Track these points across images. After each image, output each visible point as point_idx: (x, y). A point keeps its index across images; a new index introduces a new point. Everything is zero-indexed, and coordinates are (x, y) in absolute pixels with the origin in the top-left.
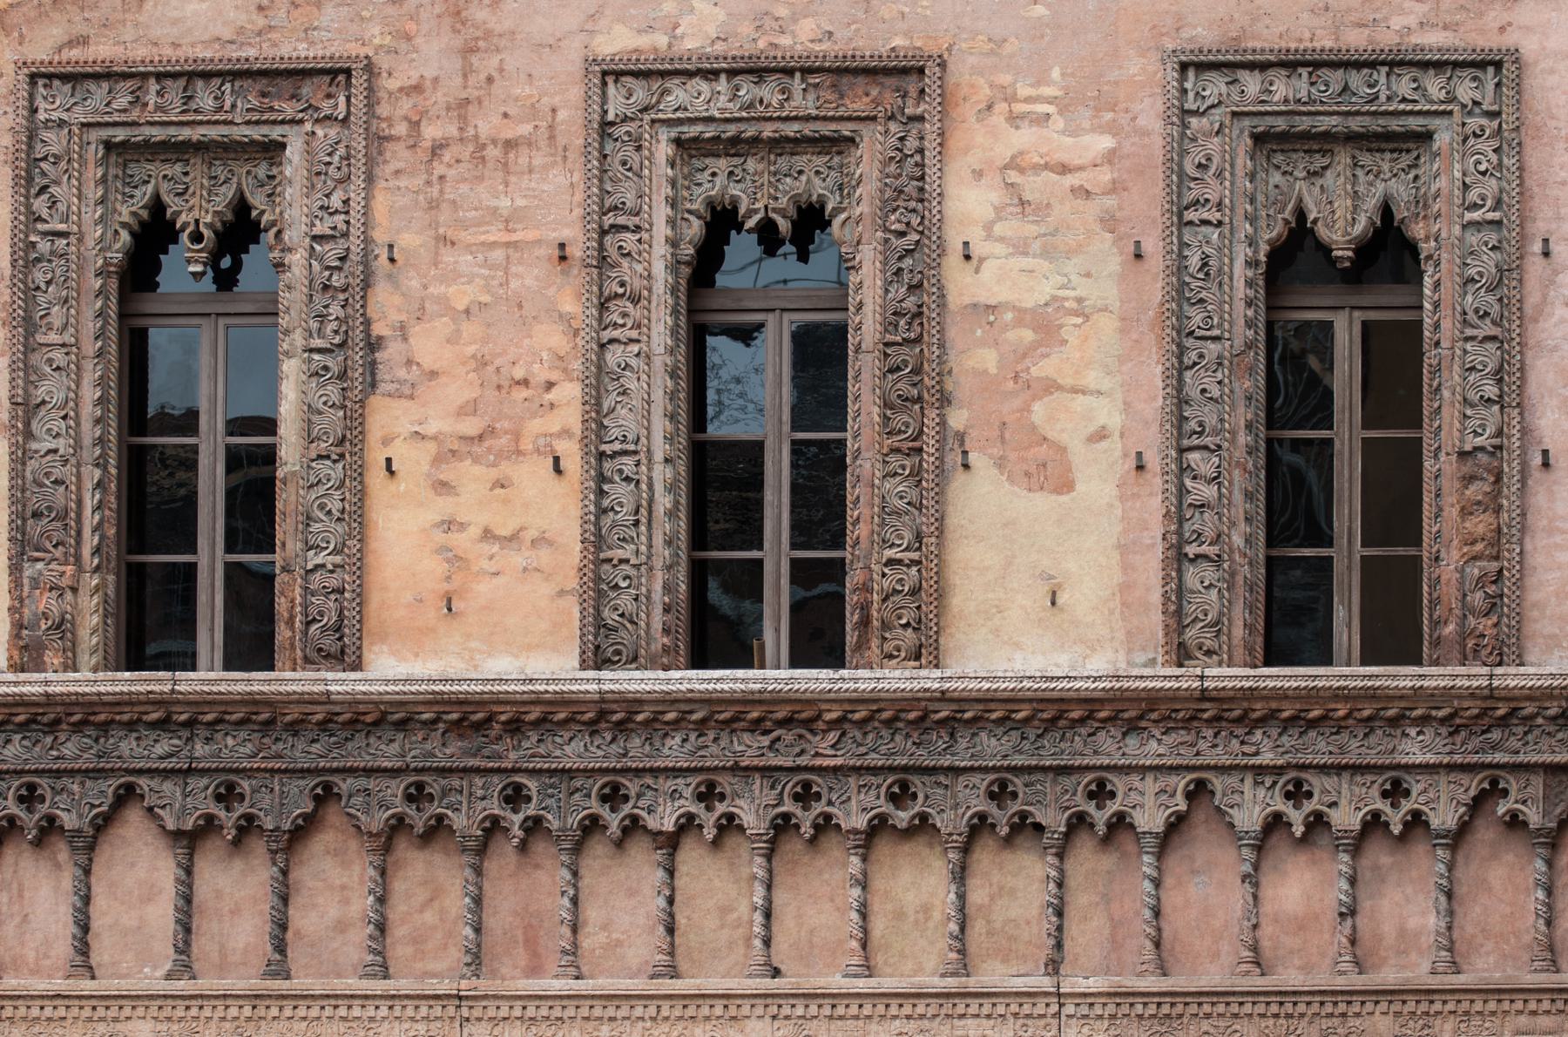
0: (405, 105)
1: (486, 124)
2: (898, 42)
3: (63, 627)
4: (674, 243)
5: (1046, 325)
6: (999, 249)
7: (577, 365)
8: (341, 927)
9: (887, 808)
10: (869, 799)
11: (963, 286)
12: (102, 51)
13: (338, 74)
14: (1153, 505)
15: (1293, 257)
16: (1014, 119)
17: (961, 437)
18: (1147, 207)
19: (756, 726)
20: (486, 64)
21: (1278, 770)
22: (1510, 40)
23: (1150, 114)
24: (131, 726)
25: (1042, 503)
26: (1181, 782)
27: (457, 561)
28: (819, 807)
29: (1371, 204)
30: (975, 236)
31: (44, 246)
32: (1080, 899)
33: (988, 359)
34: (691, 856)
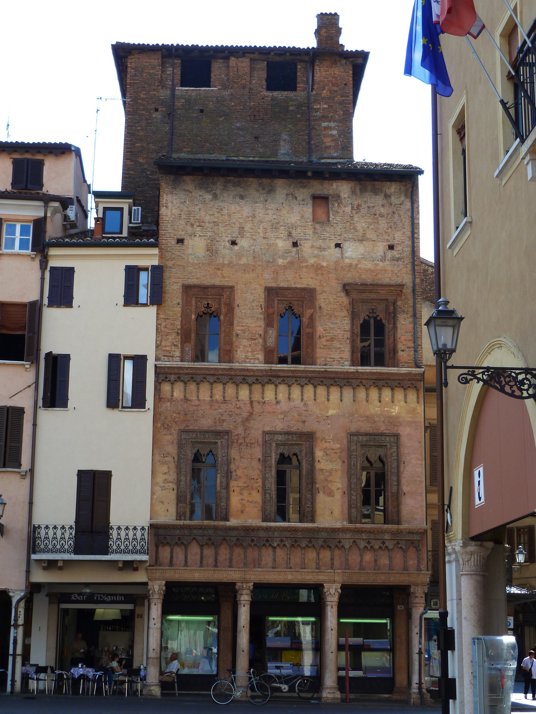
0: (236, 437)
1: (248, 440)
2: (309, 430)
3: (184, 514)
4: (275, 458)
5: (330, 472)
6: (323, 461)
7: (261, 476)
8: (225, 559)
9: (308, 544)
11: (318, 466)
12: (191, 428)
14: (346, 499)
16: (326, 442)
17: (318, 488)
18: (344, 455)
19: (289, 531)
20: (248, 432)
21: (366, 539)
22: (398, 432)
23: (345, 442)
24: (195, 529)
26: (352, 541)
27: (243, 505)
28: (298, 543)
29: (378, 455)
30: (320, 459)
32: (336, 558)
33: (322, 477)
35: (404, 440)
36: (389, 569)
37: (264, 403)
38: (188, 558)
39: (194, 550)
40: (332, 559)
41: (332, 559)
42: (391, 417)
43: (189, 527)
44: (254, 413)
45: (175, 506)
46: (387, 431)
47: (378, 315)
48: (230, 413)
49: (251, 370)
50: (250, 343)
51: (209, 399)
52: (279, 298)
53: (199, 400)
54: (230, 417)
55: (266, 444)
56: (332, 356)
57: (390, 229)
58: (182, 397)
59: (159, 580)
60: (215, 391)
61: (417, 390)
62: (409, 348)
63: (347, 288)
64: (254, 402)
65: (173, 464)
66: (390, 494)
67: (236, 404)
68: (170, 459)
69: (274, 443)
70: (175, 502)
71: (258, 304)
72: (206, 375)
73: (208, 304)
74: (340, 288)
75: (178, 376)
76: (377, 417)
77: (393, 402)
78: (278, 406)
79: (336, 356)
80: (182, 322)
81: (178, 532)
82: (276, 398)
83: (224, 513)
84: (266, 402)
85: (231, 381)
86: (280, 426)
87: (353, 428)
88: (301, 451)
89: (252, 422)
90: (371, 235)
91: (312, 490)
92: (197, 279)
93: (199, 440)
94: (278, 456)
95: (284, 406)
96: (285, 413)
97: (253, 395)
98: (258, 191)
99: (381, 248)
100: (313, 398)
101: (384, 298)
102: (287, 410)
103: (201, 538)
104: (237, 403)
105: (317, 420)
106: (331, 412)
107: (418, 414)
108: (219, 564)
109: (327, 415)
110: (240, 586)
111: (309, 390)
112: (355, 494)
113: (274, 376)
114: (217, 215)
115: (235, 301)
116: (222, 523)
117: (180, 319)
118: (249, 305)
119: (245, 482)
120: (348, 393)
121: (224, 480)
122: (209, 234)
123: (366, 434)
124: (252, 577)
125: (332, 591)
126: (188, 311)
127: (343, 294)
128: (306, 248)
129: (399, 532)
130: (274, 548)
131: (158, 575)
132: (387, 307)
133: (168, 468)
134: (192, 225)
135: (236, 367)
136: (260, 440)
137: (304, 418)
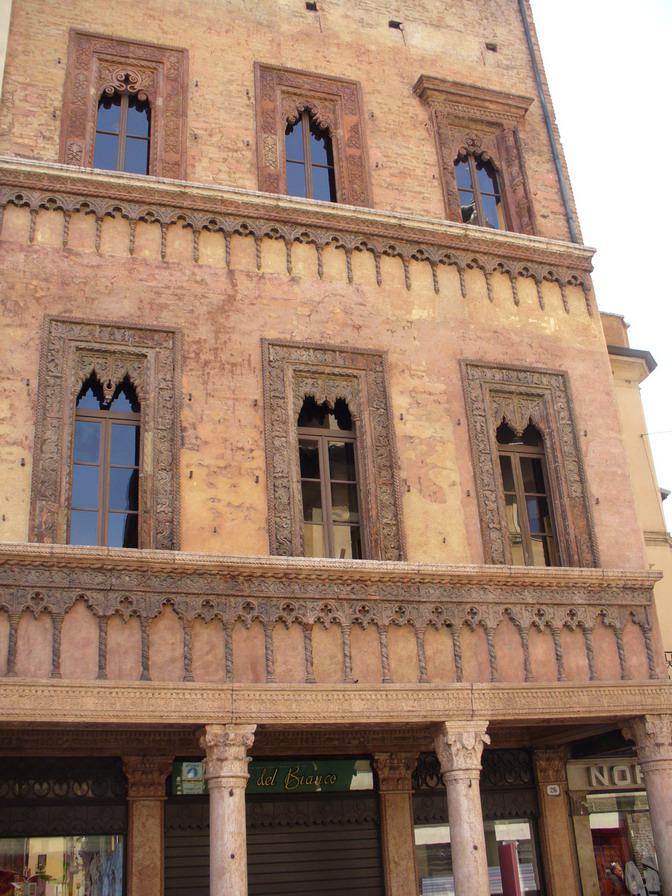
0: (194, 347)
1: (224, 357)
2: (371, 347)
4: (294, 404)
5: (431, 444)
6: (412, 418)
8: (172, 660)
9: (395, 616)
10: (389, 613)
11: (400, 429)
12: (77, 315)
13: (171, 333)
15: (505, 433)
17: (405, 481)
18: (458, 407)
20: (224, 337)
22: (563, 368)
23: (456, 379)
24: (84, 569)
25: (435, 507)
26: (501, 609)
27: (218, 514)
29: (527, 417)
31: (52, 381)
32: (466, 654)
34: (317, 634)
35: (576, 386)
36: (591, 679)
37: (262, 277)
38: (64, 656)
39: (81, 628)
40: (457, 656)
41: (457, 656)
43: (68, 565)
44: (239, 297)
45: (26, 507)
46: (540, 365)
47: (484, 152)
48: (179, 292)
49: (231, 203)
50: (224, 155)
51: (126, 255)
52: (285, 88)
53: (101, 255)
54: (180, 299)
55: (269, 368)
56: (406, 205)
57: (485, 21)
58: (58, 243)
60: (140, 241)
61: (584, 290)
62: (555, 213)
63: (422, 90)
64: (237, 275)
65: (25, 397)
66: (566, 501)
67: (194, 274)
68: (19, 385)
69: (291, 368)
70: (27, 496)
71: (240, 88)
72: (121, 200)
73: (127, 76)
74: (407, 91)
75: (49, 195)
76: (516, 334)
77: (542, 307)
78: (296, 288)
79: (416, 206)
80: (64, 95)
81: (33, 577)
82: (289, 270)
83: (167, 533)
84: (267, 276)
85: (181, 223)
86: (301, 332)
87: (471, 352)
88: (356, 393)
89: (234, 317)
90: (450, 20)
91: (392, 483)
92: (104, 25)
93: (97, 346)
94: (301, 403)
95: (309, 288)
96: (314, 306)
97: (233, 259)
100: (374, 280)
101: (494, 120)
102: (317, 299)
103: (100, 596)
104: (196, 270)
105: (388, 327)
106: (417, 314)
107: (595, 337)
108: (153, 673)
109: (408, 317)
110: (216, 736)
111: (364, 261)
112: (493, 498)
115: (191, 77)
116: (164, 555)
117: (61, 90)
118: (221, 88)
119: (221, 457)
120: (448, 277)
121: (164, 446)
123: (501, 368)
124: (254, 707)
125: (469, 741)
126: (81, 78)
127: (415, 102)
129: (604, 587)
130: (307, 628)
132: (501, 140)
133: (12, 406)
135: (195, 191)
136: (256, 359)
137: (358, 321)
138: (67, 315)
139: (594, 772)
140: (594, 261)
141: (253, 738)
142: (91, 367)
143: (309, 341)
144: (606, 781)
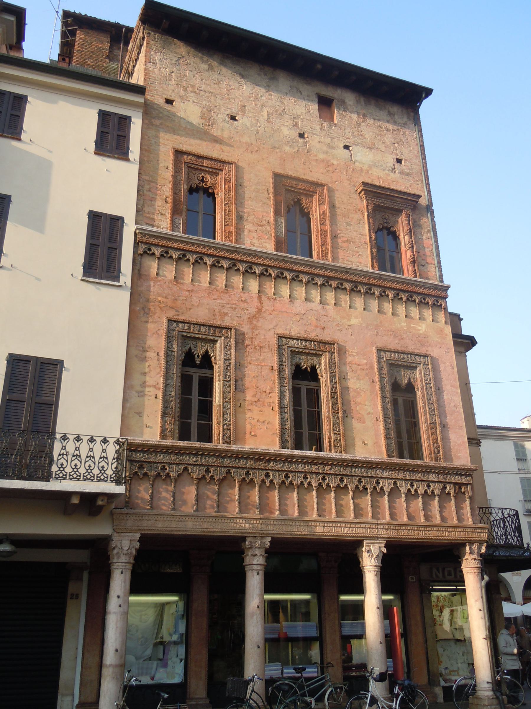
1: (256, 342)
12: (182, 318)
20: (256, 332)
29: (407, 378)
42: (419, 336)
44: (264, 310)
54: (234, 310)
56: (350, 259)
59: (131, 531)
71: (264, 187)
73: (203, 177)
89: (261, 321)
94: (294, 368)
98: (259, 74)
99: (390, 160)
106: (353, 321)
113: (288, 270)
114: (213, 86)
122: (204, 103)
123: (395, 352)
128: (314, 141)
131: (130, 523)
134: (185, 90)
138: (176, 317)
139: (434, 570)
140: (449, 292)
141: (268, 544)
142: (189, 346)
143: (298, 335)
144: (440, 576)
